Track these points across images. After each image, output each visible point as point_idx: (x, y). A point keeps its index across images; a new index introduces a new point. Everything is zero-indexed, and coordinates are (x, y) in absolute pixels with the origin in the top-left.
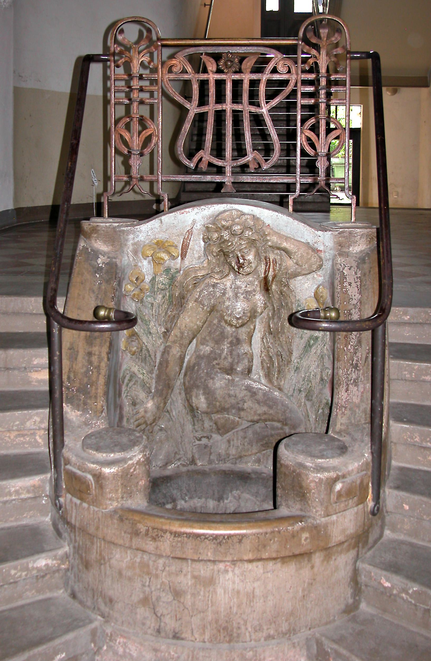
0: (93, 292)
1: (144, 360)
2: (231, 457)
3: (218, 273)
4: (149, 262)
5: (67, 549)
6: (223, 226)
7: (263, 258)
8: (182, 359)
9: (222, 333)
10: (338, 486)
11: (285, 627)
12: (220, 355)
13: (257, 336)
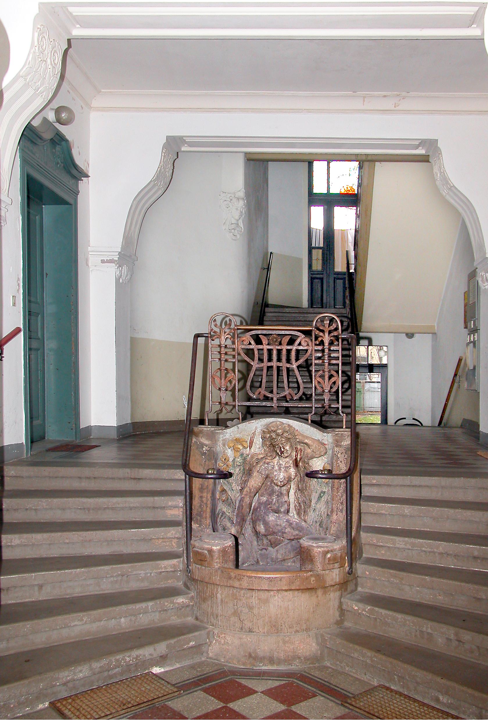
0: (202, 465)
1: (229, 505)
2: (279, 560)
3: (269, 456)
4: (232, 450)
5: (193, 594)
6: (272, 430)
7: (294, 448)
8: (251, 504)
9: (273, 490)
10: (329, 555)
11: (304, 627)
12: (272, 502)
13: (292, 492)
